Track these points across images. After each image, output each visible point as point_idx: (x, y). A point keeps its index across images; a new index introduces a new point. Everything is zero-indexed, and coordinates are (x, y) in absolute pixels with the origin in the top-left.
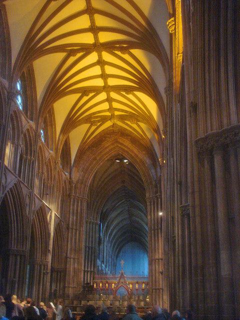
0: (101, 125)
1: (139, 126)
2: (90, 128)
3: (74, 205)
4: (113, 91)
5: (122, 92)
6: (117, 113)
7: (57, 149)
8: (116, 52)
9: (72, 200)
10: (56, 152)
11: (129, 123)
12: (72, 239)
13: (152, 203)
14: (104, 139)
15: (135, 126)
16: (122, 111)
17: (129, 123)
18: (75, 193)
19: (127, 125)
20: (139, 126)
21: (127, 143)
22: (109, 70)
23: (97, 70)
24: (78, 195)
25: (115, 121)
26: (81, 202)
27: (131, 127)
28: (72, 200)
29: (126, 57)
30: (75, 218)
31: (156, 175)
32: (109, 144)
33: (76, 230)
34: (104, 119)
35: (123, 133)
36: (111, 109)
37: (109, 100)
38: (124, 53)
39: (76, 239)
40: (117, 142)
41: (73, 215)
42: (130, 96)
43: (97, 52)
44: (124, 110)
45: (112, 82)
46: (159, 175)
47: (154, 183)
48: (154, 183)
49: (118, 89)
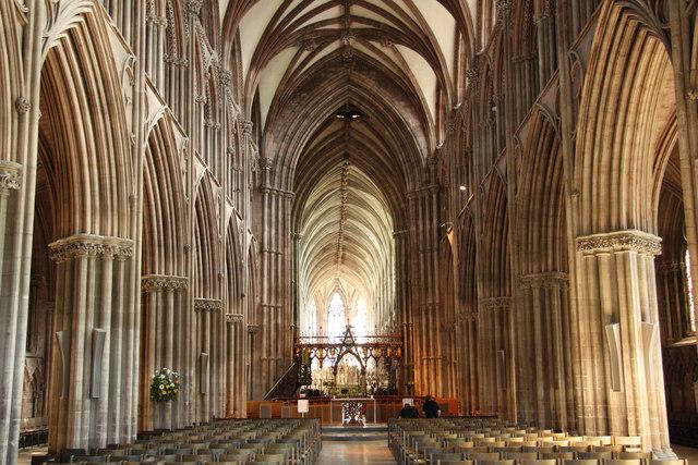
0: (320, 49)
1: (396, 51)
3: (270, 207)
6: (355, 25)
7: (245, 101)
10: (244, 107)
13: (420, 203)
14: (323, 75)
15: (388, 52)
16: (369, 21)
17: (377, 45)
18: (272, 183)
19: (373, 48)
21: (370, 83)
24: (276, 187)
25: (351, 41)
26: (283, 201)
27: (380, 53)
32: (333, 86)
33: (277, 254)
35: (363, 64)
40: (349, 81)
44: (372, 21)
46: (433, 148)
47: (424, 163)
48: (424, 163)
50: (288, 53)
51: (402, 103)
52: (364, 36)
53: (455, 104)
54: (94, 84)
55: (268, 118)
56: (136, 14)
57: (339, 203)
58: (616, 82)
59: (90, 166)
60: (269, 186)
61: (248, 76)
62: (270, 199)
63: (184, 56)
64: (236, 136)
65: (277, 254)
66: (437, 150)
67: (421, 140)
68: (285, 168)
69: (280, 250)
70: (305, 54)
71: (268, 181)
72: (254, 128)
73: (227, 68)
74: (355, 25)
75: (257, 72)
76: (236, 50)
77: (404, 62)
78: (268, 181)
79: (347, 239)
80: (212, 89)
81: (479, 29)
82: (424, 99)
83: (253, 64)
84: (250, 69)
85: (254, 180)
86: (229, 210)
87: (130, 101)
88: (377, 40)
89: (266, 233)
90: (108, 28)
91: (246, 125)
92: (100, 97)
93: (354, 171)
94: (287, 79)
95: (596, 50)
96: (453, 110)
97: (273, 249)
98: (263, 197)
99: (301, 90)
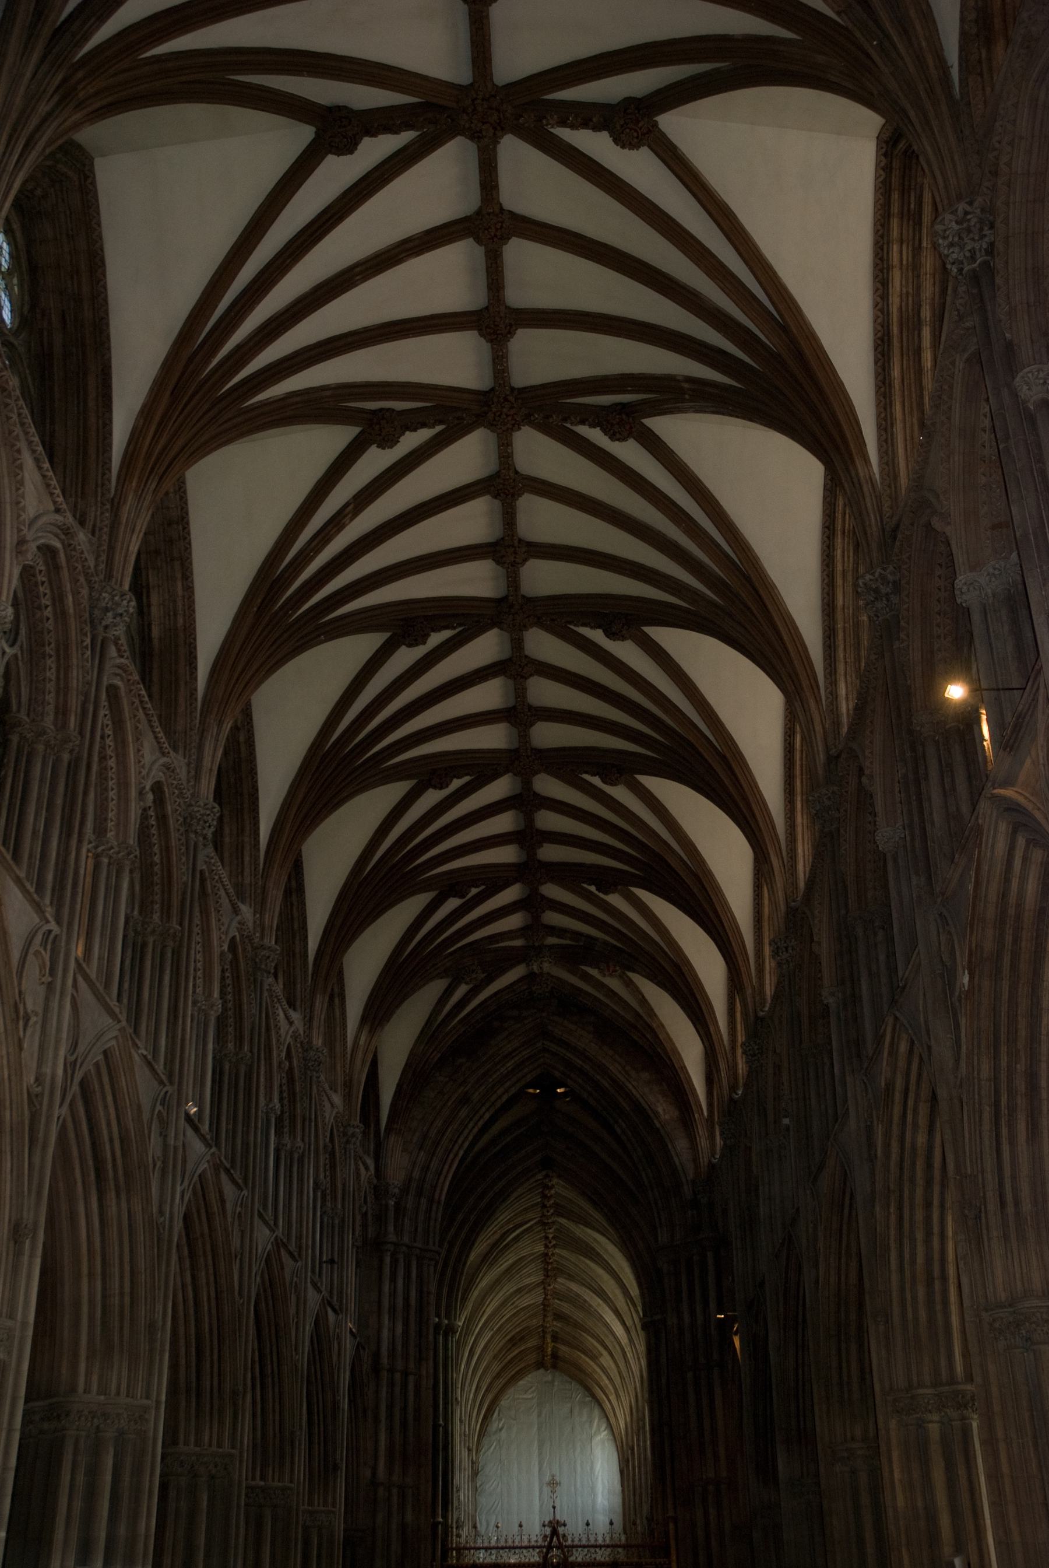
0: (490, 980)
1: (629, 984)
3: (393, 1279)
4: (553, 880)
6: (552, 940)
7: (348, 1085)
9: (388, 1260)
10: (348, 1097)
11: (594, 972)
12: (390, 1407)
15: (614, 983)
16: (577, 935)
17: (594, 972)
19: (586, 977)
22: (549, 820)
23: (503, 823)
24: (406, 1239)
25: (546, 966)
28: (388, 1260)
30: (399, 1329)
31: (695, 1160)
33: (406, 1374)
34: (509, 959)
36: (534, 928)
38: (613, 784)
39: (404, 1409)
41: (393, 1318)
42: (615, 899)
46: (704, 1161)
50: (435, 988)
51: (645, 1076)
53: (733, 1088)
54: (108, 1147)
55: (394, 1105)
56: (176, 1017)
57: (540, 1248)
58: (921, 1139)
59: (91, 1275)
60: (392, 1237)
61: (357, 1038)
62: (395, 1262)
63: (246, 1048)
64: (332, 1154)
65: (406, 1374)
66: (712, 1166)
67: (680, 1145)
68: (424, 1201)
69: (412, 1365)
70: (462, 990)
71: (391, 1228)
72: (365, 1134)
73: (318, 1041)
74: (552, 940)
75: (372, 1032)
76: (337, 996)
77: (643, 1001)
78: (391, 1228)
79: (559, 1316)
80: (291, 1080)
81: (760, 969)
82: (684, 1068)
83: (364, 1019)
85: (365, 1226)
86: (313, 1298)
87: (159, 1164)
89: (385, 1333)
90: (137, 1058)
91: (351, 1131)
92: (114, 1165)
93: (560, 1188)
94: (429, 1034)
96: (731, 1099)
97: (399, 1364)
98: (381, 1261)
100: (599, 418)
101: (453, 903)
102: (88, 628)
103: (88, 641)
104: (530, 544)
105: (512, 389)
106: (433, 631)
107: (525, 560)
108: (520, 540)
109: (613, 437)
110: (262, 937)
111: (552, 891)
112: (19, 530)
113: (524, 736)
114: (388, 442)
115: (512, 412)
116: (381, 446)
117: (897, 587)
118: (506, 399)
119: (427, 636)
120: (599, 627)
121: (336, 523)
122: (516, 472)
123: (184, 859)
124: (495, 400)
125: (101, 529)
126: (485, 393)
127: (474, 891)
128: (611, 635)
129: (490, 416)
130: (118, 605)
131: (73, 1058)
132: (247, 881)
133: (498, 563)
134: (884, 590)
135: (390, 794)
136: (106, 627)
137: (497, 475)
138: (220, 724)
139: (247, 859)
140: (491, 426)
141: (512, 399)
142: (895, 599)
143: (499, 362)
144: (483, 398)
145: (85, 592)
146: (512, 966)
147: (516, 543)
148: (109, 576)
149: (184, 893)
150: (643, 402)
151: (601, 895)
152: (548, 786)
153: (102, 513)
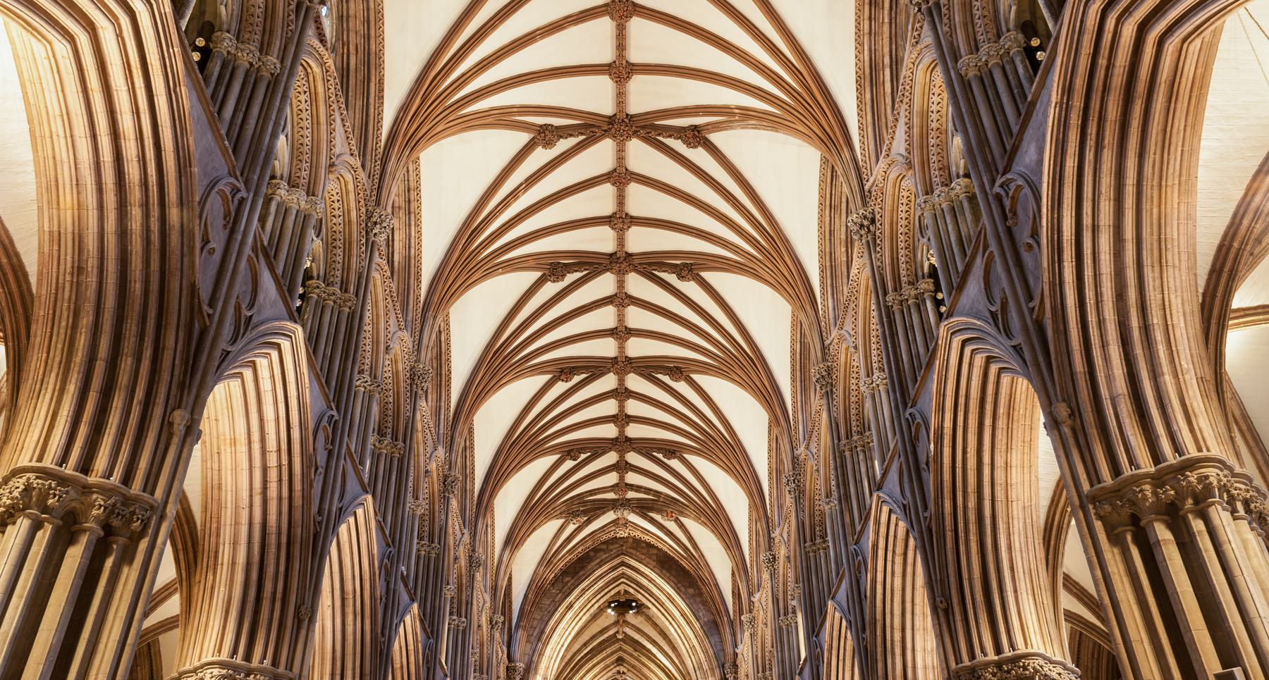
0: (589, 522)
1: (682, 526)
2: (561, 529)
4: (634, 450)
5: (655, 454)
6: (631, 495)
8: (660, 376)
11: (657, 517)
14: (592, 554)
15: (672, 526)
16: (648, 491)
17: (657, 517)
20: (682, 526)
29: (682, 387)
34: (603, 507)
37: (622, 467)
42: (675, 463)
43: (617, 373)
44: (651, 490)
45: (634, 431)
49: (647, 447)
50: (552, 526)
52: (643, 508)
75: (512, 552)
84: (504, 549)
88: (659, 511)
94: (547, 560)
95: (873, 546)
99: (564, 573)
100: (679, 133)
101: (569, 464)
102: (364, 233)
103: (364, 241)
104: (632, 217)
105: (627, 115)
106: (569, 273)
107: (629, 227)
108: (626, 214)
109: (689, 145)
110: (450, 469)
111: (633, 458)
112: (331, 158)
113: (621, 348)
114: (548, 144)
115: (626, 129)
116: (544, 147)
117: (873, 221)
118: (623, 121)
119: (564, 276)
120: (674, 273)
121: (514, 195)
122: (627, 170)
123: (409, 401)
124: (617, 121)
125: (374, 175)
126: (610, 117)
127: (583, 456)
128: (681, 277)
129: (613, 130)
130: (382, 221)
131: (341, 506)
132: (441, 432)
133: (612, 228)
134: (866, 223)
135: (533, 383)
136: (375, 234)
137: (615, 170)
138: (435, 318)
139: (442, 417)
140: (614, 137)
141: (626, 120)
142: (872, 228)
143: (621, 97)
144: (611, 120)
145: (363, 210)
146: (604, 513)
147: (624, 216)
148: (378, 203)
149: (407, 423)
150: (708, 124)
151: (665, 460)
152: (635, 382)
153: (375, 166)
